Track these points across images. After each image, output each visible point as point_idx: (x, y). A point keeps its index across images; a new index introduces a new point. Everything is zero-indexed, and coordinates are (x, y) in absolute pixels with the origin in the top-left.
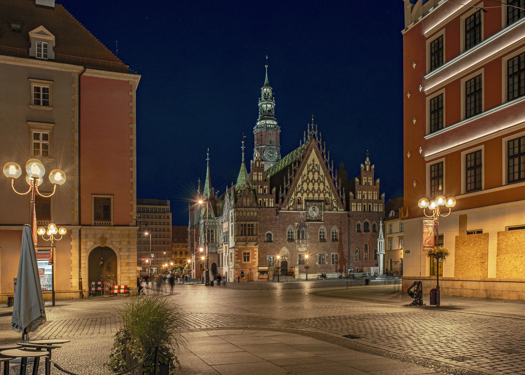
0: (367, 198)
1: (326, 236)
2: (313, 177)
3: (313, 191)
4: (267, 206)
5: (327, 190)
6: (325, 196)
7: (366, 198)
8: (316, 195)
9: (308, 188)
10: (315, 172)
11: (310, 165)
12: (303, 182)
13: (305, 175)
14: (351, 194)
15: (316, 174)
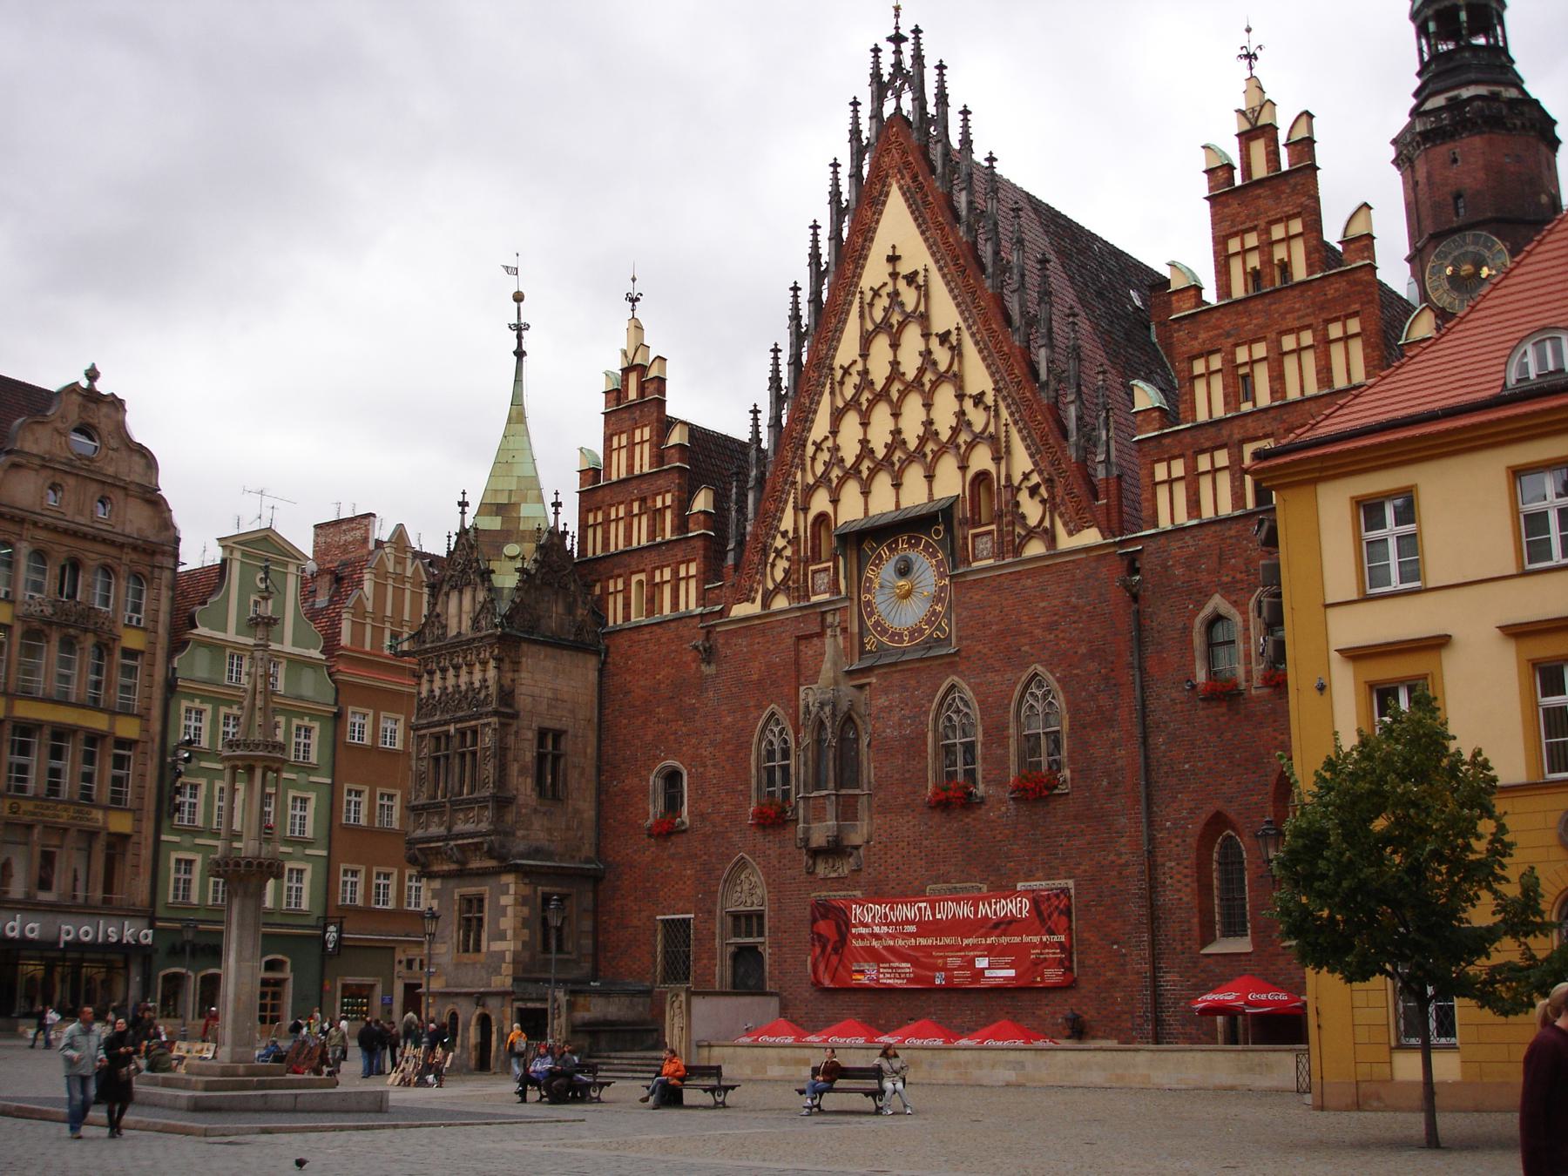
0: (1272, 392)
1: (979, 747)
2: (895, 364)
3: (893, 461)
4: (667, 610)
5: (978, 418)
6: (963, 468)
7: (1264, 399)
8: (914, 476)
9: (864, 442)
10: (902, 325)
11: (876, 293)
12: (837, 416)
13: (846, 371)
14: (1146, 396)
15: (912, 338)
